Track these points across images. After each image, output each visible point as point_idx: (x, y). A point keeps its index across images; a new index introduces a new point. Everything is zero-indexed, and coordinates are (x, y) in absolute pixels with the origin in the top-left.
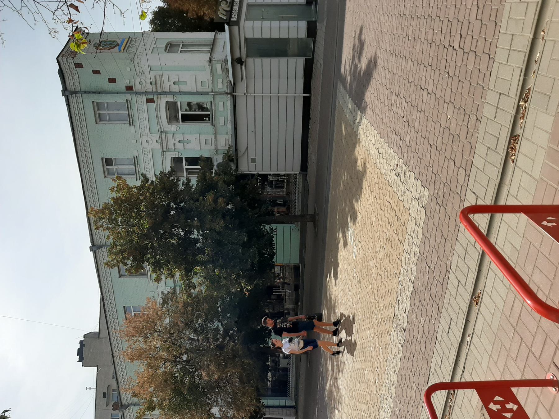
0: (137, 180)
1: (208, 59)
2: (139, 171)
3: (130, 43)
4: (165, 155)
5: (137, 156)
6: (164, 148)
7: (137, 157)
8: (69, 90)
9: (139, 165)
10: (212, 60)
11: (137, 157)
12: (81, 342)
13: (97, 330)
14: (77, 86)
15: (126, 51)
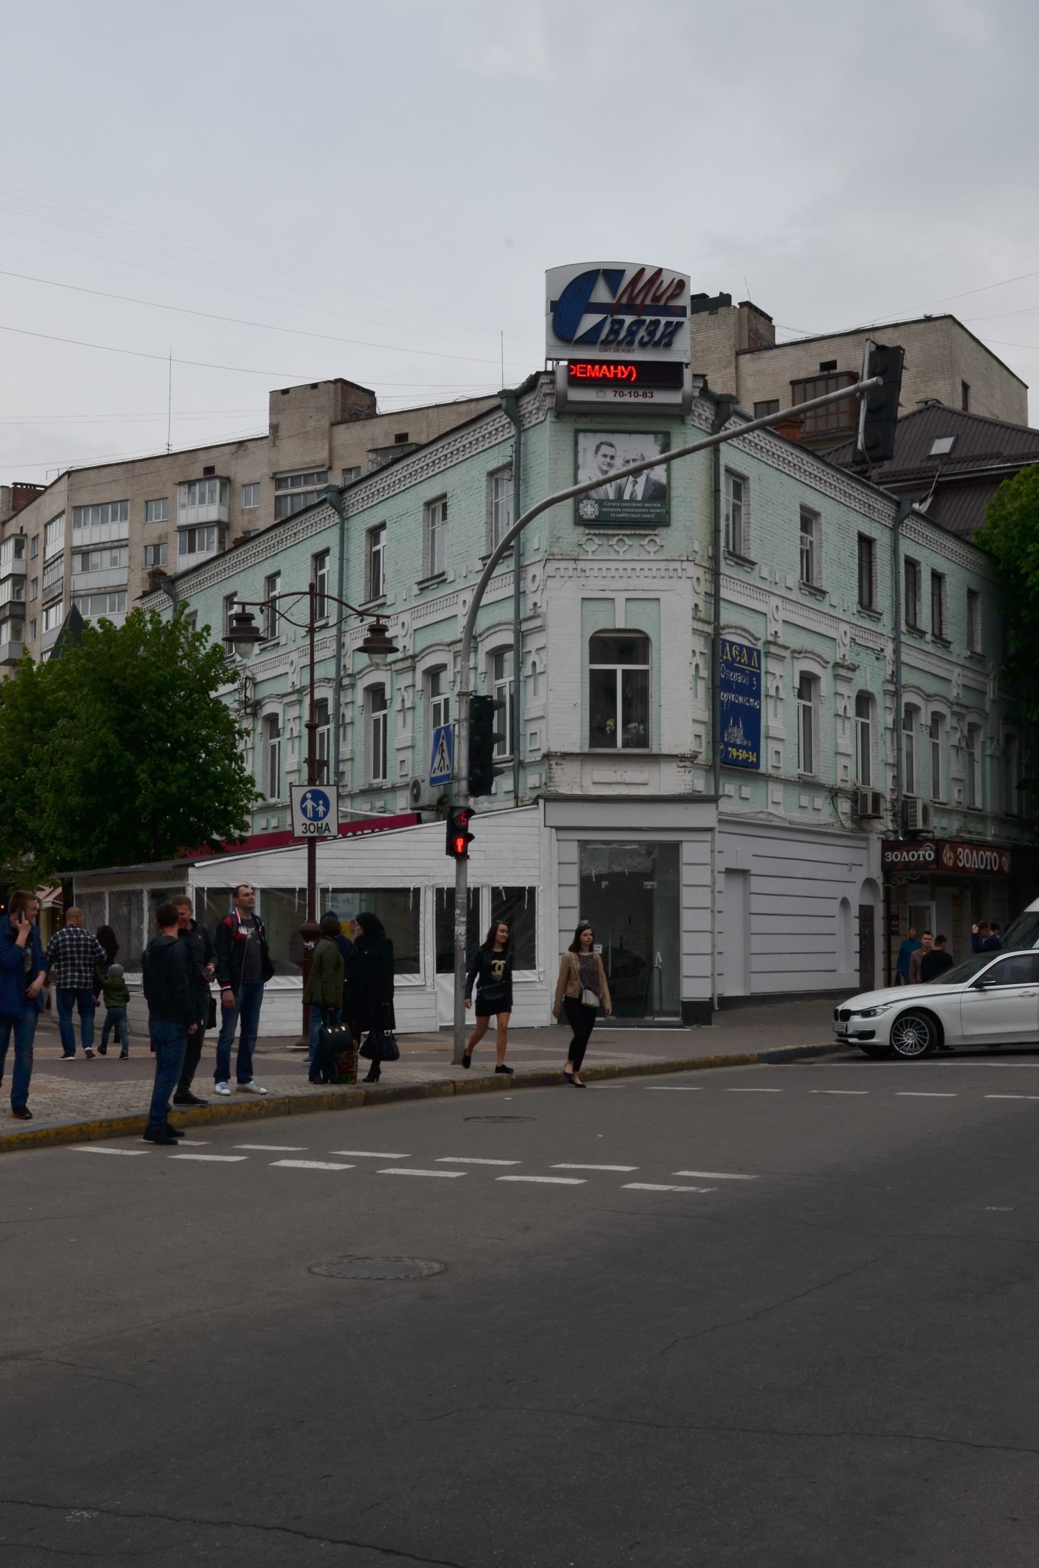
0: (419, 583)
1: (553, 749)
2: (431, 588)
3: (626, 535)
4: (447, 648)
5: (448, 581)
6: (455, 646)
7: (446, 580)
8: (521, 404)
9: (436, 586)
10: (549, 760)
11: (446, 580)
12: (725, 299)
13: (779, 340)
14: (529, 420)
15: (588, 534)
